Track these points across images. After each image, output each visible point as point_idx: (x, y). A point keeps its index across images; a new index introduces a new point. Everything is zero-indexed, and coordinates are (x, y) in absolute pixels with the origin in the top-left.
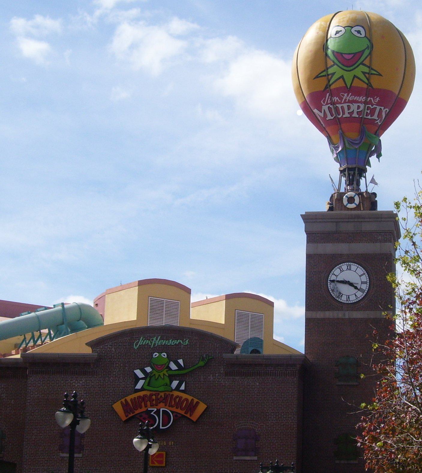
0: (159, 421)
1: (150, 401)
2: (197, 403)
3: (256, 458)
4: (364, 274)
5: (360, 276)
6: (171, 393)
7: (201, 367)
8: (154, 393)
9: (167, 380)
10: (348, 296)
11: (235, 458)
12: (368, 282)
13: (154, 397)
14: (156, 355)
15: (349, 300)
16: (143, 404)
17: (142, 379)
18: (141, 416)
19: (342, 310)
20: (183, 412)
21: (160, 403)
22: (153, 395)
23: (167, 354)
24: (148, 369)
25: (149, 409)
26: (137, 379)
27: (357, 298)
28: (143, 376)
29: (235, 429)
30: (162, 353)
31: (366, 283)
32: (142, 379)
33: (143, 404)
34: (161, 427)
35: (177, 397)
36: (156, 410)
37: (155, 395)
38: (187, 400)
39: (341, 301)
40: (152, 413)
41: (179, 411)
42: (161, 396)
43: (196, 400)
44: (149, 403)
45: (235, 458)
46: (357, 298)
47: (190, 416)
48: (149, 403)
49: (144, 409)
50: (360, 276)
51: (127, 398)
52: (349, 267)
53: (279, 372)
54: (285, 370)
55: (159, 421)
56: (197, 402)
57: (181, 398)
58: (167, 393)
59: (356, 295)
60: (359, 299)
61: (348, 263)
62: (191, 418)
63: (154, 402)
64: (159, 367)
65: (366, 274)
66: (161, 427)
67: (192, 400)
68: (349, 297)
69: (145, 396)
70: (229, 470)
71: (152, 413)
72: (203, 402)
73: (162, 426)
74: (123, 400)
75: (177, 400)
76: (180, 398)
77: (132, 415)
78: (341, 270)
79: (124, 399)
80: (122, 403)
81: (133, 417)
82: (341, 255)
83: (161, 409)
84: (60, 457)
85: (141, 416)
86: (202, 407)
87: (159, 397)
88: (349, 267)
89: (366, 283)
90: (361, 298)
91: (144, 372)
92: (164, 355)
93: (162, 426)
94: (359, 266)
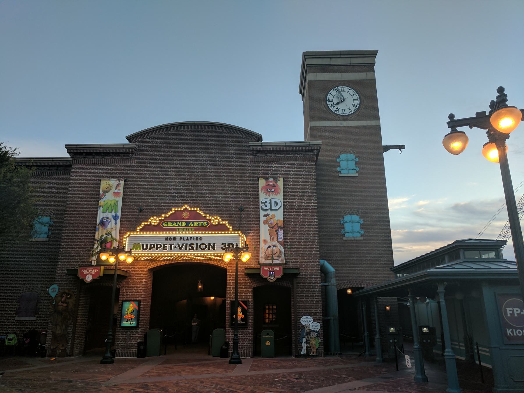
5: (352, 96)
10: (343, 110)
12: (359, 99)
15: (344, 113)
19: (339, 120)
27: (351, 111)
31: (357, 100)
39: (338, 113)
46: (351, 111)
50: (352, 96)
52: (342, 89)
53: (299, 158)
59: (350, 109)
60: (353, 112)
61: (342, 87)
65: (357, 94)
68: (344, 111)
78: (330, 100)
82: (336, 81)
88: (342, 89)
89: (357, 100)
90: (354, 111)
94: (351, 89)
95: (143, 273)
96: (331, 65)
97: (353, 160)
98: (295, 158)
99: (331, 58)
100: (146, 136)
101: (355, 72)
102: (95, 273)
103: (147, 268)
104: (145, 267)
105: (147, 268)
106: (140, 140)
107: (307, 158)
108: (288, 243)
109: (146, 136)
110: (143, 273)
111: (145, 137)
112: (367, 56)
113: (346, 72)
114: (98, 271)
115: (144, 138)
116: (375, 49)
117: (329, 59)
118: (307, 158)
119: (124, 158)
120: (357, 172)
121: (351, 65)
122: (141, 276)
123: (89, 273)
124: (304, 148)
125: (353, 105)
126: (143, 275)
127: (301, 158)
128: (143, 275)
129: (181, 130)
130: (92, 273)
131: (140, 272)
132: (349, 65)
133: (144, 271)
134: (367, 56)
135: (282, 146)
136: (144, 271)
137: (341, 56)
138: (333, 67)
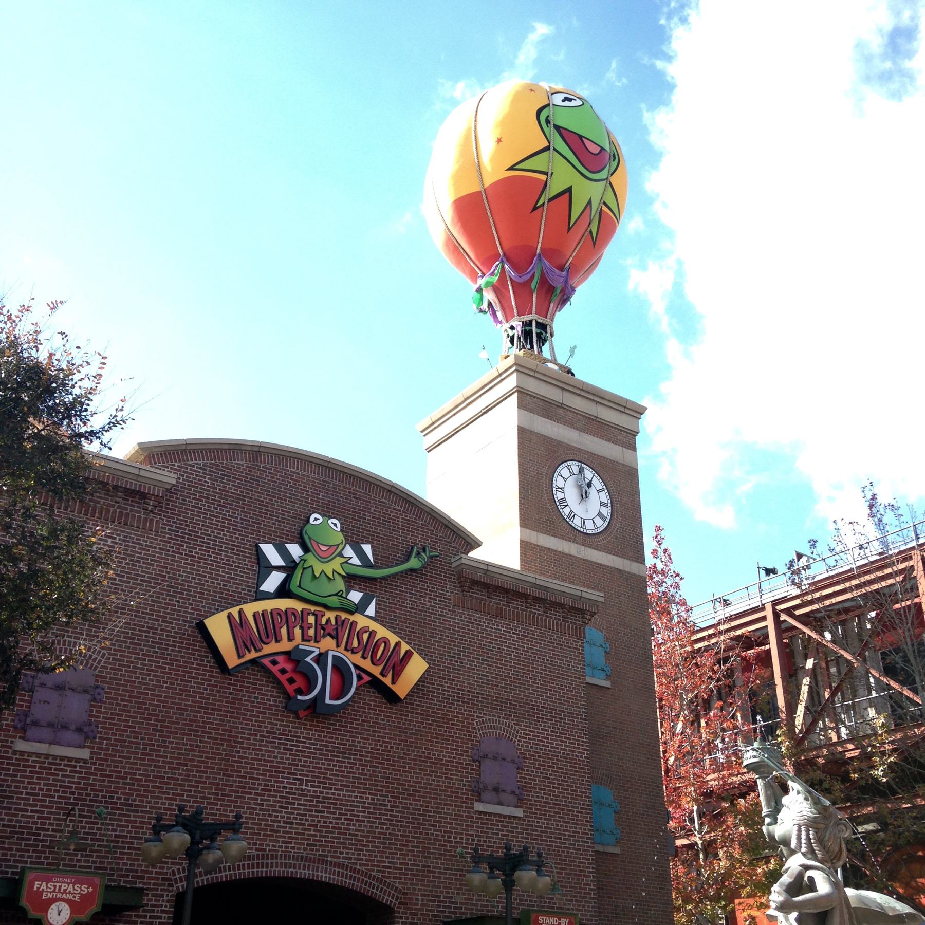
0: (326, 681)
1: (301, 627)
2: (408, 654)
3: (519, 813)
6: (352, 618)
7: (412, 571)
8: (313, 608)
9: (340, 585)
11: (479, 807)
13: (311, 620)
14: (316, 519)
16: (284, 631)
17: (278, 568)
18: (274, 663)
19: (575, 542)
20: (376, 671)
21: (324, 636)
22: (309, 614)
23: (341, 524)
24: (295, 550)
25: (301, 647)
26: (266, 568)
28: (282, 563)
29: (476, 733)
30: (330, 518)
32: (278, 568)
33: (284, 631)
34: (328, 701)
35: (365, 630)
36: (317, 652)
37: (314, 614)
38: (386, 641)
40: (308, 659)
41: (367, 664)
42: (328, 621)
43: (405, 647)
44: (297, 631)
45: (479, 807)
47: (393, 683)
48: (297, 631)
49: (285, 646)
51: (244, 607)
54: (563, 621)
55: (326, 681)
56: (407, 651)
57: (372, 634)
58: (344, 616)
62: (393, 688)
63: (311, 632)
64: (324, 548)
66: (328, 701)
67: (398, 645)
69: (294, 612)
70: (465, 838)
71: (308, 659)
72: (420, 654)
73: (331, 699)
74: (235, 611)
75: (365, 636)
76: (371, 633)
77: (253, 655)
79: (236, 609)
80: (230, 617)
81: (253, 662)
82: (570, 448)
83: (331, 654)
84: (15, 752)
85: (274, 663)
86: (416, 667)
87: (324, 621)
91: (284, 554)
92: (335, 525)
93: (331, 699)
95: (162, 906)
96: (561, 406)
97: (601, 646)
98: (546, 620)
99: (563, 389)
100: (196, 460)
101: (602, 437)
102: (82, 896)
103: (175, 888)
104: (170, 885)
105: (175, 888)
106: (176, 464)
107: (569, 626)
108: (534, 848)
109: (196, 460)
110: (162, 906)
111: (192, 461)
112: (626, 411)
114: (91, 890)
115: (190, 463)
116: (643, 403)
118: (569, 626)
119: (126, 509)
120: (608, 677)
121: (597, 421)
122: (156, 914)
123: (59, 895)
124: (568, 602)
125: (600, 514)
126: (163, 912)
127: (557, 623)
128: (163, 912)
129: (291, 472)
130: (70, 897)
131: (151, 900)
132: (593, 420)
133: (165, 898)
134: (626, 411)
135: (527, 584)
136: (165, 898)
137: (583, 394)
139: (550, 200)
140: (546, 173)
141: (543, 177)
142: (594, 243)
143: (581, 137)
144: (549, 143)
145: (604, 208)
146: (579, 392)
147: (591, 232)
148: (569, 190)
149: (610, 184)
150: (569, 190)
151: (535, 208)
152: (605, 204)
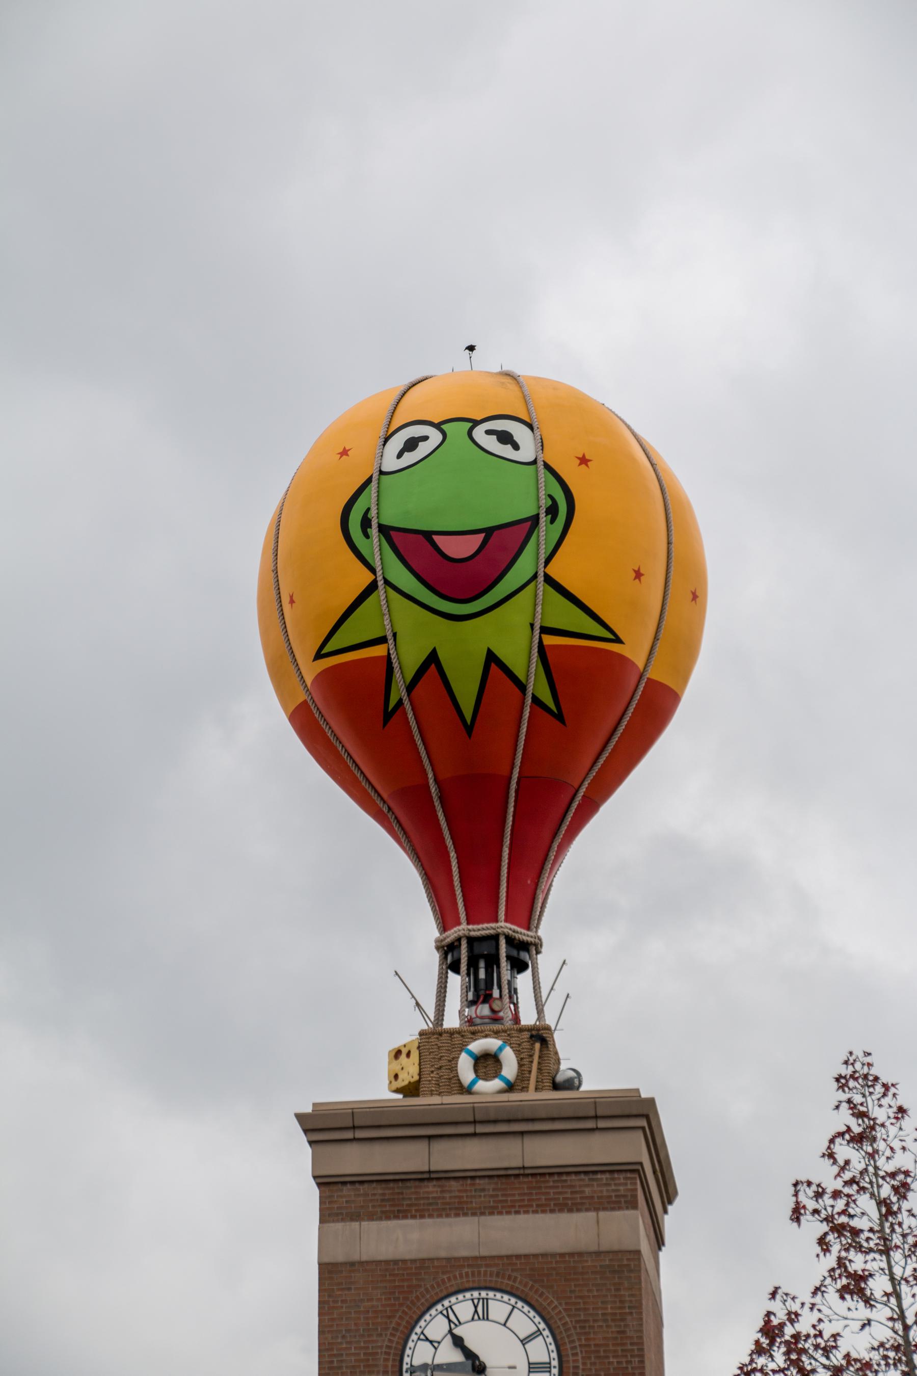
4: (539, 1333)
5: (524, 1342)
50: (524, 1342)
61: (476, 1294)
65: (546, 1333)
82: (452, 1264)
94: (520, 1304)
96: (428, 1177)
101: (542, 1208)
113: (500, 1213)
117: (422, 1146)
121: (527, 1175)
138: (440, 1183)
139: (410, 688)
140: (382, 640)
141: (379, 651)
142: (559, 717)
143: (428, 535)
144: (373, 570)
145: (549, 640)
146: (469, 1129)
147: (535, 699)
148: (433, 658)
149: (549, 580)
150: (433, 658)
151: (388, 716)
152: (545, 630)
